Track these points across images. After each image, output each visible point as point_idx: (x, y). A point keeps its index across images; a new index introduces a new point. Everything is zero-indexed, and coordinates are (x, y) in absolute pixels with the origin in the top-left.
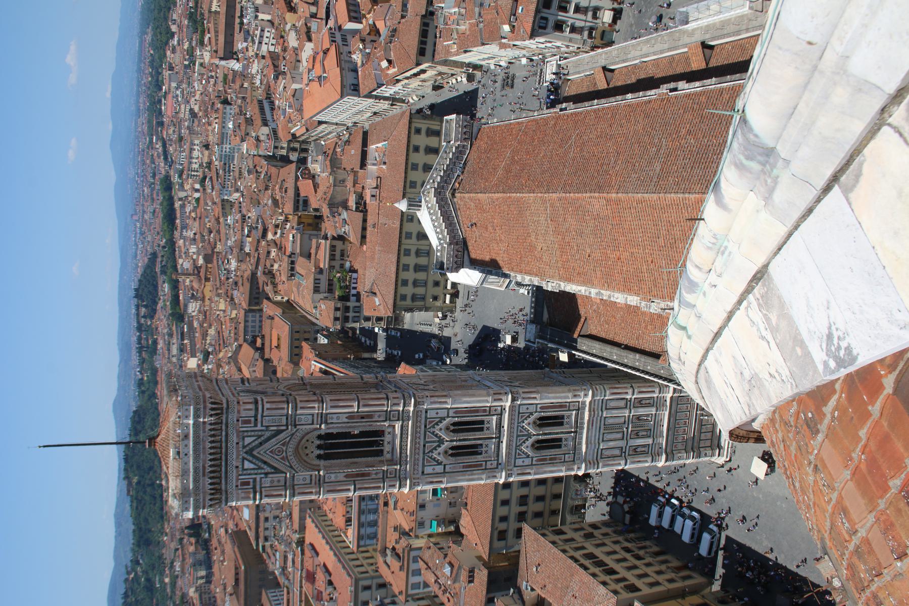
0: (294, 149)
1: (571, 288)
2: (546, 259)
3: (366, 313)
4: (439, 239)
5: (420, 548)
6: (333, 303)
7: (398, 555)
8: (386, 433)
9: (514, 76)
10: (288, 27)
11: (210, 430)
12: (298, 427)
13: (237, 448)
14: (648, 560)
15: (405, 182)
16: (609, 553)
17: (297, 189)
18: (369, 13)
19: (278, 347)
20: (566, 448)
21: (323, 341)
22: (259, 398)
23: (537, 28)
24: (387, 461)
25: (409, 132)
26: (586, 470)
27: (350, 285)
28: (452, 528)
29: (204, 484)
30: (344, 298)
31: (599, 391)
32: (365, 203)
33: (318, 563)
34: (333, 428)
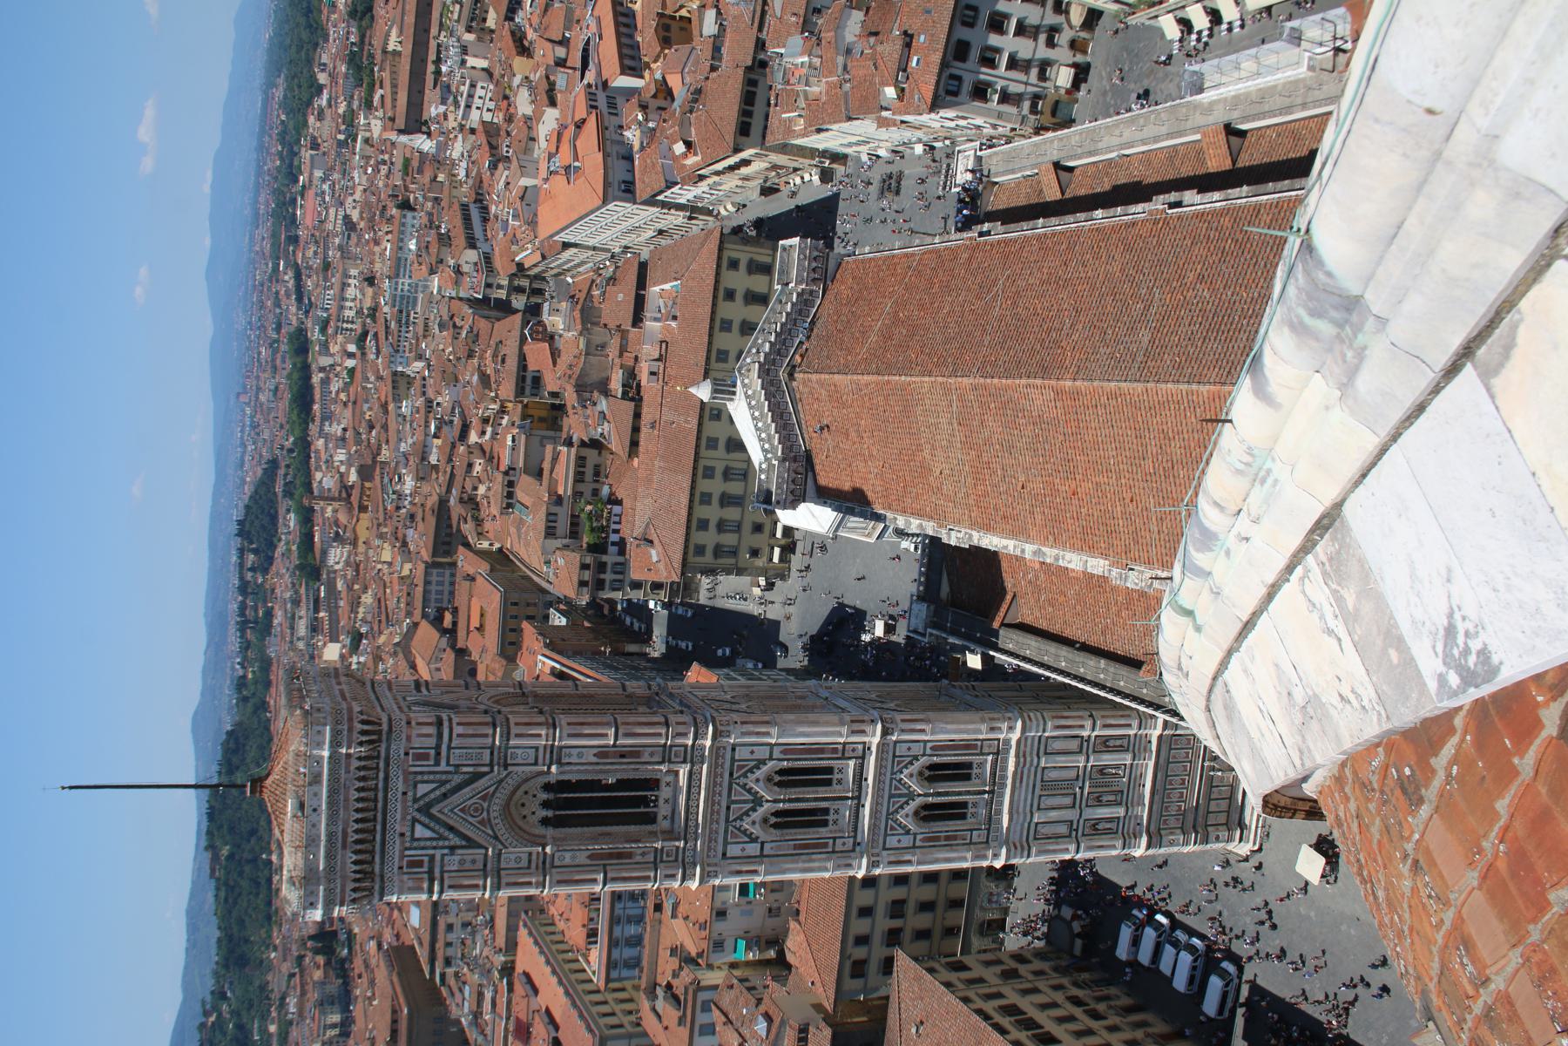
1: (990, 541)
2: (948, 490)
3: (635, 575)
4: (764, 450)
5: (715, 987)
7: (676, 998)
8: (663, 784)
9: (900, 176)
10: (517, 80)
11: (359, 769)
12: (510, 769)
13: (404, 802)
14: (1113, 1020)
15: (709, 351)
16: (1044, 1007)
17: (522, 358)
19: (480, 629)
20: (973, 820)
22: (445, 717)
24: (663, 832)
25: (719, 266)
26: (1008, 858)
27: (608, 526)
28: (772, 954)
29: (344, 863)
30: (598, 548)
31: (1035, 722)
32: (639, 386)
34: (571, 772)
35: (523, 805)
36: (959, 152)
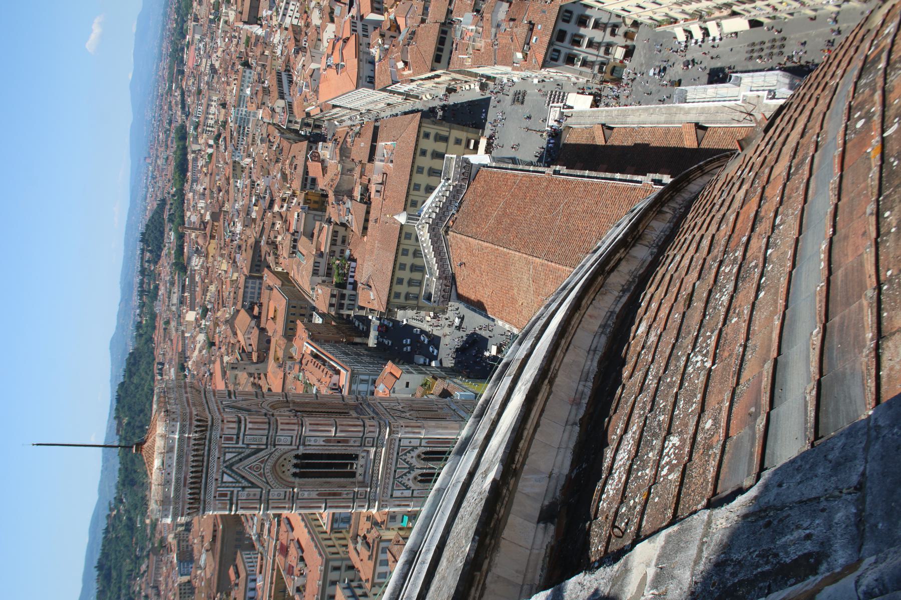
0: (308, 125)
3: (361, 303)
5: (390, 540)
6: (330, 290)
7: (368, 544)
8: (360, 458)
9: (525, 93)
10: (313, 4)
11: (194, 445)
12: (277, 447)
13: (218, 463)
15: (409, 184)
18: (391, 8)
19: (274, 319)
21: (318, 320)
22: (243, 418)
24: (359, 482)
25: (418, 136)
27: (348, 274)
29: (184, 494)
30: (341, 285)
32: (369, 196)
33: (292, 538)
35: (283, 466)
36: (551, 107)
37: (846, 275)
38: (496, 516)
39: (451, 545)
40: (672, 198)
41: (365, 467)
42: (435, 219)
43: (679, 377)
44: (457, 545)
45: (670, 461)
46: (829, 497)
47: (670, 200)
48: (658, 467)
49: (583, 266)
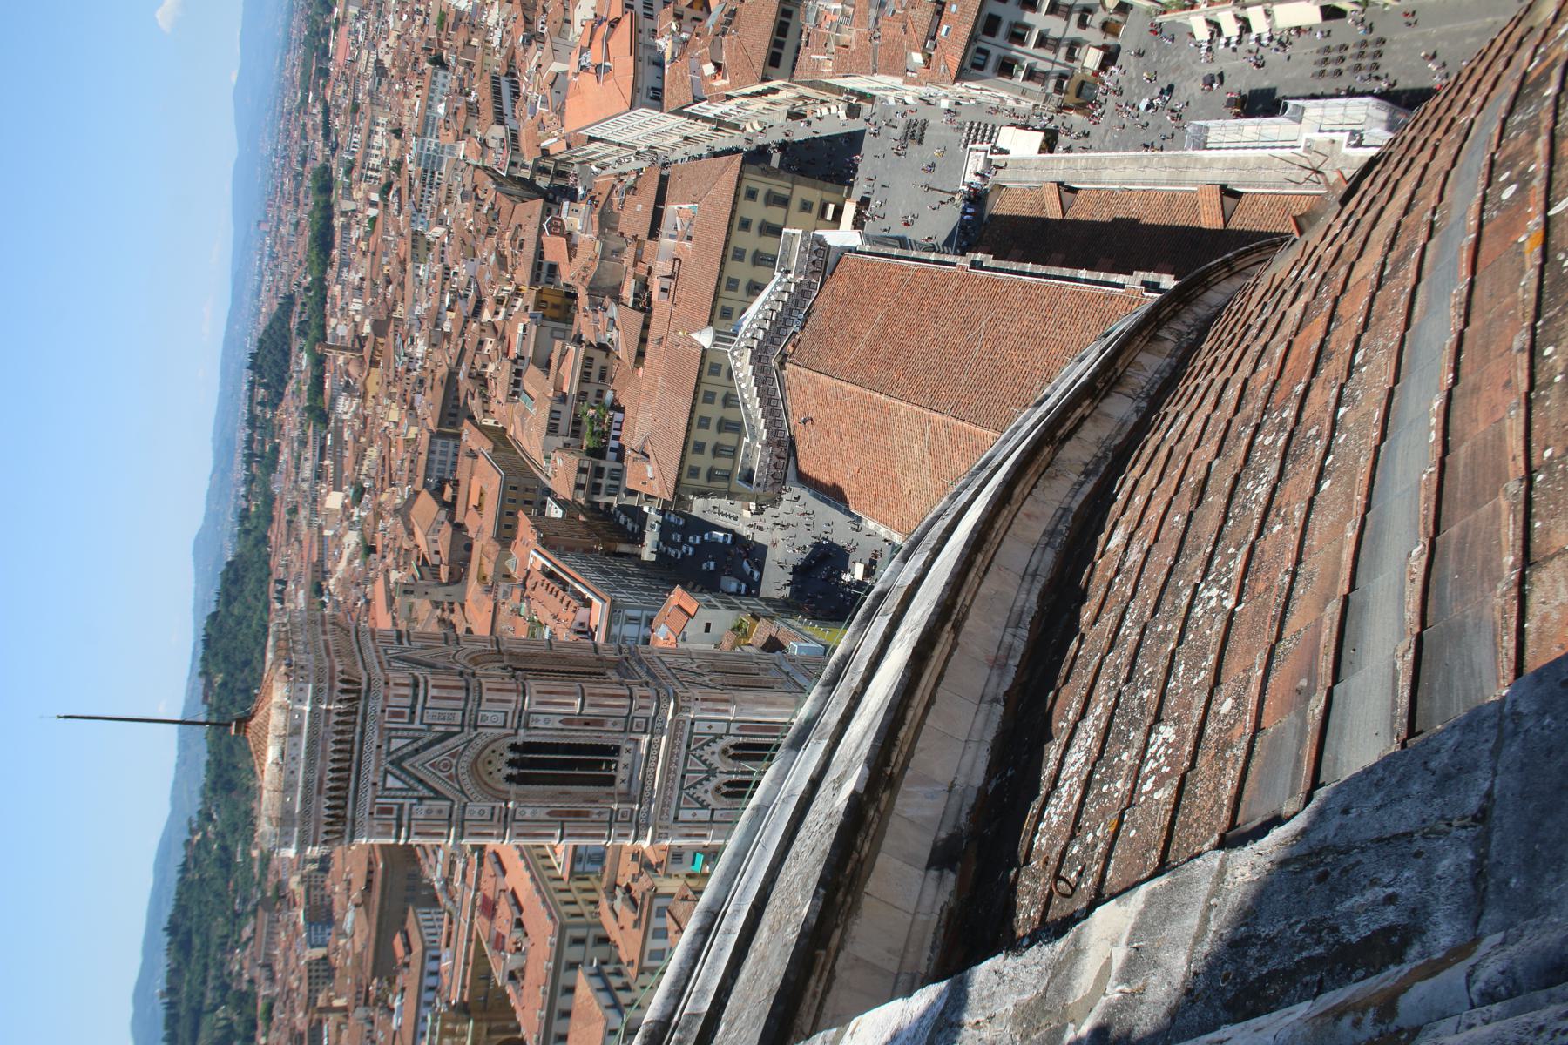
0: (545, 171)
3: (630, 483)
5: (671, 895)
6: (577, 459)
7: (633, 900)
8: (623, 751)
9: (925, 125)
11: (337, 723)
12: (480, 730)
13: (378, 754)
19: (478, 508)
21: (555, 512)
22: (421, 680)
23: (969, 67)
24: (620, 794)
25: (736, 195)
27: (608, 432)
29: (318, 808)
30: (597, 453)
32: (649, 298)
35: (490, 762)
37: (1473, 455)
38: (855, 855)
39: (778, 903)
40: (1175, 314)
41: (632, 767)
42: (763, 341)
43: (1179, 624)
44: (787, 903)
45: (1159, 768)
46: (1430, 833)
47: (1170, 318)
48: (1137, 777)
49: (1018, 428)
